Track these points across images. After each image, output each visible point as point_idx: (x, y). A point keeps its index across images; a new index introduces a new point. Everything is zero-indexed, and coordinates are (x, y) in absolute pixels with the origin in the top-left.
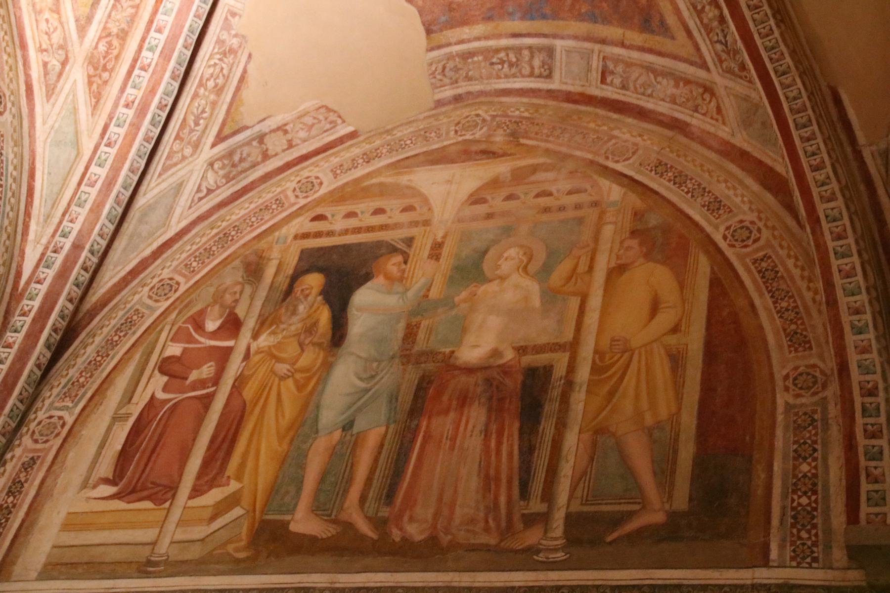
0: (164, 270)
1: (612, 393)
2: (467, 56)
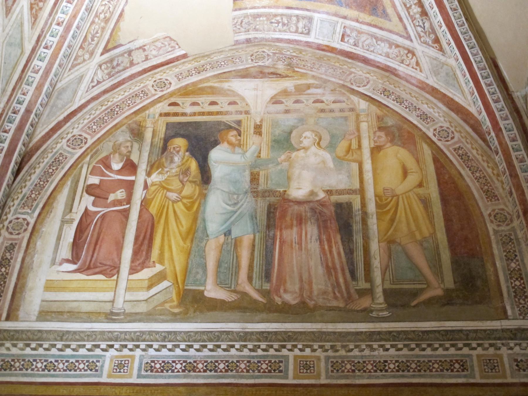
1: (392, 220)
2: (256, 16)
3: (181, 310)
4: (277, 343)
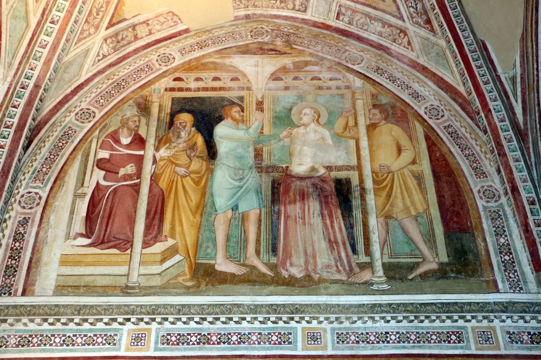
1: (389, 196)
3: (194, 283)
4: (285, 316)
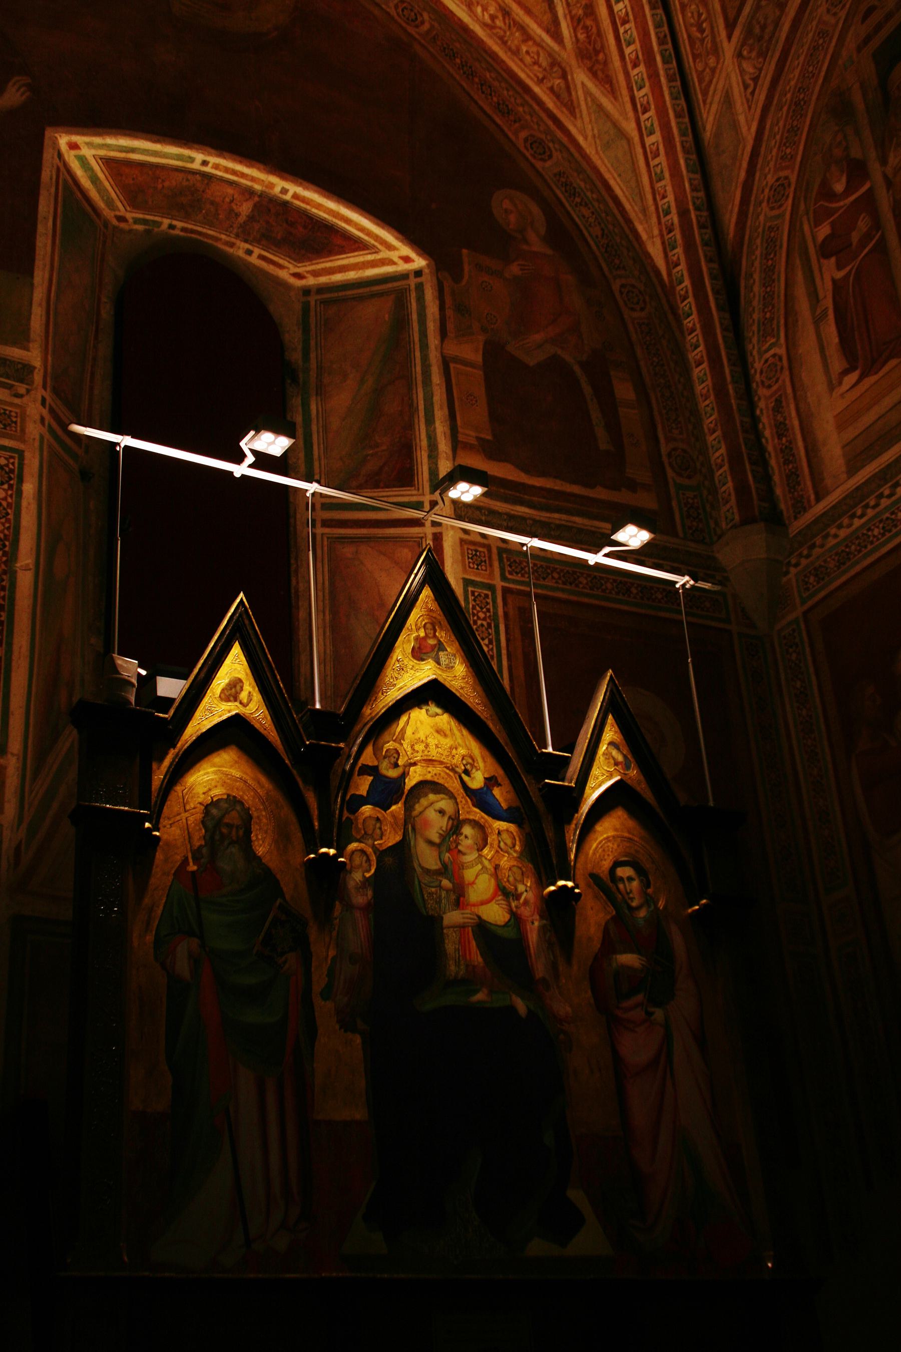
0: (767, 178)
